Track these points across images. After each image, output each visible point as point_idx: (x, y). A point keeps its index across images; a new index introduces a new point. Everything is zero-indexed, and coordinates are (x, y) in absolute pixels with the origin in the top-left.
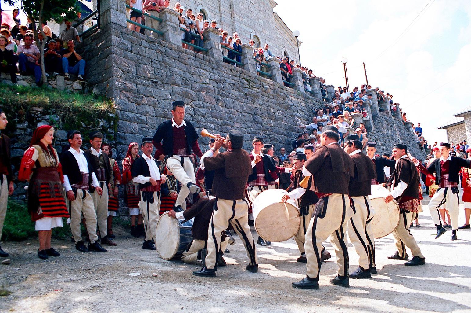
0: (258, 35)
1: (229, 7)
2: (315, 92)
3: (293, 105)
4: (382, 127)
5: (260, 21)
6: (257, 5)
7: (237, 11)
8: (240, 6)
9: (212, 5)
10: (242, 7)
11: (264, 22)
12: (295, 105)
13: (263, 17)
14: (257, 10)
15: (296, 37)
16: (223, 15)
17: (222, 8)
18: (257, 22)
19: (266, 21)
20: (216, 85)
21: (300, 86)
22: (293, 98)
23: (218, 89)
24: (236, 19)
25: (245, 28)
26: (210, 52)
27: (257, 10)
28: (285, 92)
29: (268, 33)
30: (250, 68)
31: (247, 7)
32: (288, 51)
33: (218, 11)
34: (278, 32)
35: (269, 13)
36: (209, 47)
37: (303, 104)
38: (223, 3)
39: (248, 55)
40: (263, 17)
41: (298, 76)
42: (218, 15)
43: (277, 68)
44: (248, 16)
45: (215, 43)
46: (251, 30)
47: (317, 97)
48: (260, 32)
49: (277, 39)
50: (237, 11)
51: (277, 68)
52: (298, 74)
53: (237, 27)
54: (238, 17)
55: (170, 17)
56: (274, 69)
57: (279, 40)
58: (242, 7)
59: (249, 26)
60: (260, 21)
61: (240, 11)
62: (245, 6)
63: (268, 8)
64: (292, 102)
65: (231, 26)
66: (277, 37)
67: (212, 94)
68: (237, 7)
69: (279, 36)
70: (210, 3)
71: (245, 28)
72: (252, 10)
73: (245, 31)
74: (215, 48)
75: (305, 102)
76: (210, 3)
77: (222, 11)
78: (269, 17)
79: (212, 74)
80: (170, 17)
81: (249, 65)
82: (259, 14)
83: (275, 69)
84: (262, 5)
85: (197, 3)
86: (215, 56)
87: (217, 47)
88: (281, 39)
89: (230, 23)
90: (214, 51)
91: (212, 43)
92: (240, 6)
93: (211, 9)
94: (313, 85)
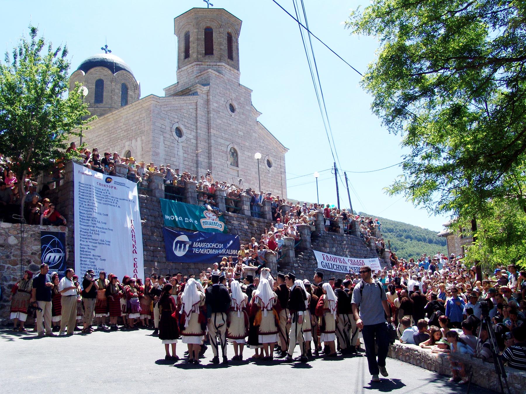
0: (236, 147)
1: (207, 122)
2: (265, 213)
3: (233, 227)
5: (239, 133)
6: (237, 117)
7: (215, 126)
8: (218, 120)
9: (189, 122)
10: (220, 122)
11: (244, 133)
12: (236, 228)
13: (244, 128)
14: (236, 122)
15: (258, 159)
16: (199, 131)
17: (199, 124)
18: (236, 134)
19: (245, 132)
20: (154, 220)
21: (245, 211)
22: (235, 222)
23: (155, 222)
24: (212, 134)
25: (222, 141)
26: (154, 191)
27: (236, 122)
28: (227, 218)
29: (247, 144)
30: (191, 201)
31: (226, 121)
32: (271, 159)
33: (194, 127)
34: (261, 141)
35: (251, 123)
36: (153, 188)
37: (246, 227)
38: (200, 120)
39: (190, 190)
40: (244, 128)
41: (244, 202)
42: (195, 130)
43: (220, 197)
44: (225, 130)
45: (158, 184)
46: (228, 143)
47: (266, 218)
48: (238, 144)
49: (259, 148)
50: (215, 126)
51: (220, 197)
53: (212, 142)
54: (215, 132)
55: (120, 170)
56: (218, 198)
57: (262, 149)
58: (220, 122)
59: (226, 139)
60: (239, 133)
61: (217, 125)
62: (224, 120)
63: (250, 119)
64: (233, 225)
65: (207, 141)
66: (260, 146)
67: (149, 228)
68: (215, 122)
69: (263, 145)
70: (186, 121)
71: (222, 141)
72: (231, 123)
73: (221, 144)
74: (158, 188)
75: (248, 225)
76: (186, 121)
77: (198, 127)
78: (250, 128)
79: (152, 211)
80: (120, 170)
81: (190, 198)
82: (239, 126)
84: (244, 117)
85: (173, 122)
86: (157, 195)
87: (160, 187)
88: (265, 148)
89: (206, 137)
90: (157, 191)
91: (156, 185)
92: (218, 120)
93: (188, 125)
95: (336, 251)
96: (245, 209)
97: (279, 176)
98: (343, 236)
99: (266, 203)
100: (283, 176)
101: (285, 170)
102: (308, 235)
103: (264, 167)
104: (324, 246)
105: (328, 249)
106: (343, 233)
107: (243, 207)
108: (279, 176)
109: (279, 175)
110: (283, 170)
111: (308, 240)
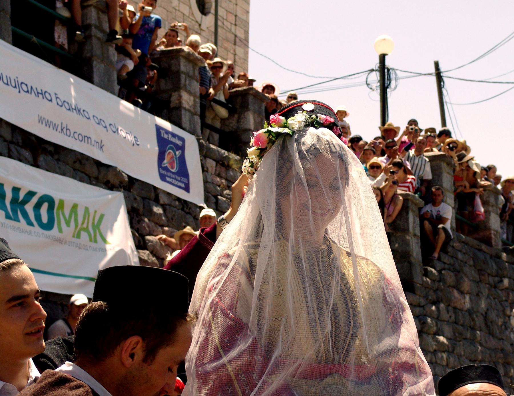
4: (457, 287)
21: (183, 112)
41: (183, 77)
52: (183, 68)
83: (94, 41)
94: (240, 114)
95: (488, 310)
96: (185, 105)
97: (226, 49)
98: (499, 257)
99: (251, 99)
100: (239, 51)
101: (247, 33)
102: (415, 235)
103: (185, 10)
104: (457, 287)
105: (467, 297)
106: (500, 247)
107: (174, 98)
108: (226, 49)
109: (230, 46)
110: (240, 34)
111: (415, 254)
